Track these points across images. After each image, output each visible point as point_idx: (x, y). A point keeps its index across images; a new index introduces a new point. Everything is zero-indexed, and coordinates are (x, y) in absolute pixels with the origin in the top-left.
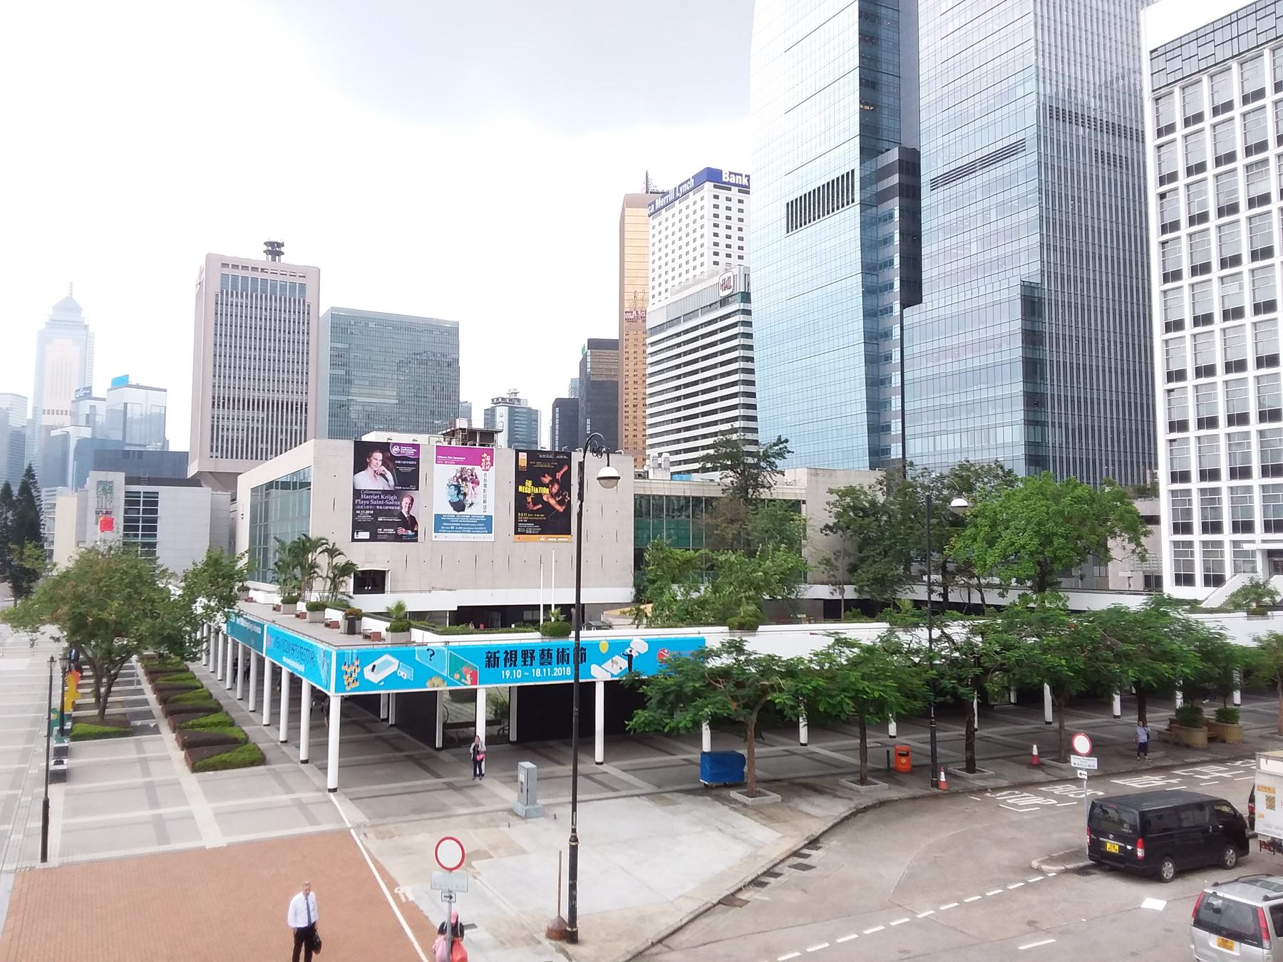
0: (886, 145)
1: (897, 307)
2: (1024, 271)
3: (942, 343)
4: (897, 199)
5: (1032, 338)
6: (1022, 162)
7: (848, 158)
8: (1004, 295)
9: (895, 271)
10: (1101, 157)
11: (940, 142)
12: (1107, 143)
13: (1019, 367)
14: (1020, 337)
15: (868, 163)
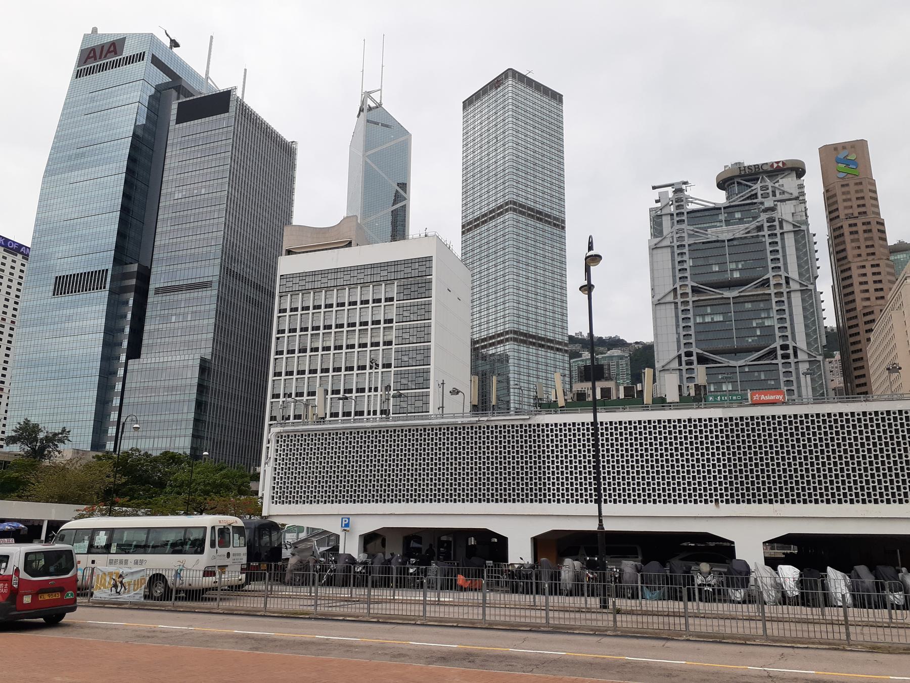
0: (129, 260)
1: (123, 358)
2: (203, 351)
3: (150, 384)
4: (133, 294)
5: (202, 388)
6: (209, 293)
7: (105, 261)
8: (190, 363)
9: (126, 336)
10: (249, 300)
11: (164, 268)
12: (252, 293)
13: (194, 404)
14: (196, 388)
15: (117, 267)
